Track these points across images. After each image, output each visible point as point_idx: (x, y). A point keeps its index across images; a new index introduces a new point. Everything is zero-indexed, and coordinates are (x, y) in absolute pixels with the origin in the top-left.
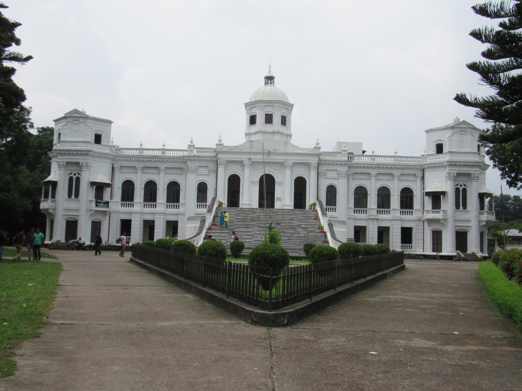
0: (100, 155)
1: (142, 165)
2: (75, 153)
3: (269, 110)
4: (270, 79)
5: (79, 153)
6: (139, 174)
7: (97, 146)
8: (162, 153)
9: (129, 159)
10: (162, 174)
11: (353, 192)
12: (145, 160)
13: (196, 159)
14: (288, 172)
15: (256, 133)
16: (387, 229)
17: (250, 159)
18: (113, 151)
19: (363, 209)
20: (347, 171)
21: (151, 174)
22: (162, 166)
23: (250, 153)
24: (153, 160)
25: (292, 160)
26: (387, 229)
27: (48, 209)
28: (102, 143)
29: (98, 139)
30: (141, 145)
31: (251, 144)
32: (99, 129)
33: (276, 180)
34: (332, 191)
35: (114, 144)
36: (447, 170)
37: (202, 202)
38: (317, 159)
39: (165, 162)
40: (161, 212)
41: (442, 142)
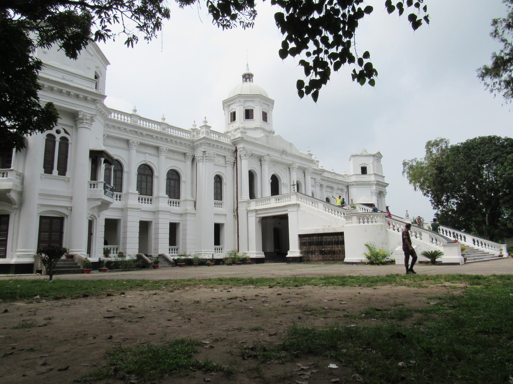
2: (73, 92)
5: (81, 95)
9: (122, 127)
10: (163, 157)
12: (145, 133)
13: (216, 144)
15: (256, 129)
21: (147, 155)
24: (155, 135)
25: (298, 163)
27: (9, 191)
36: (374, 188)
37: (217, 200)
40: (162, 209)
41: (366, 166)
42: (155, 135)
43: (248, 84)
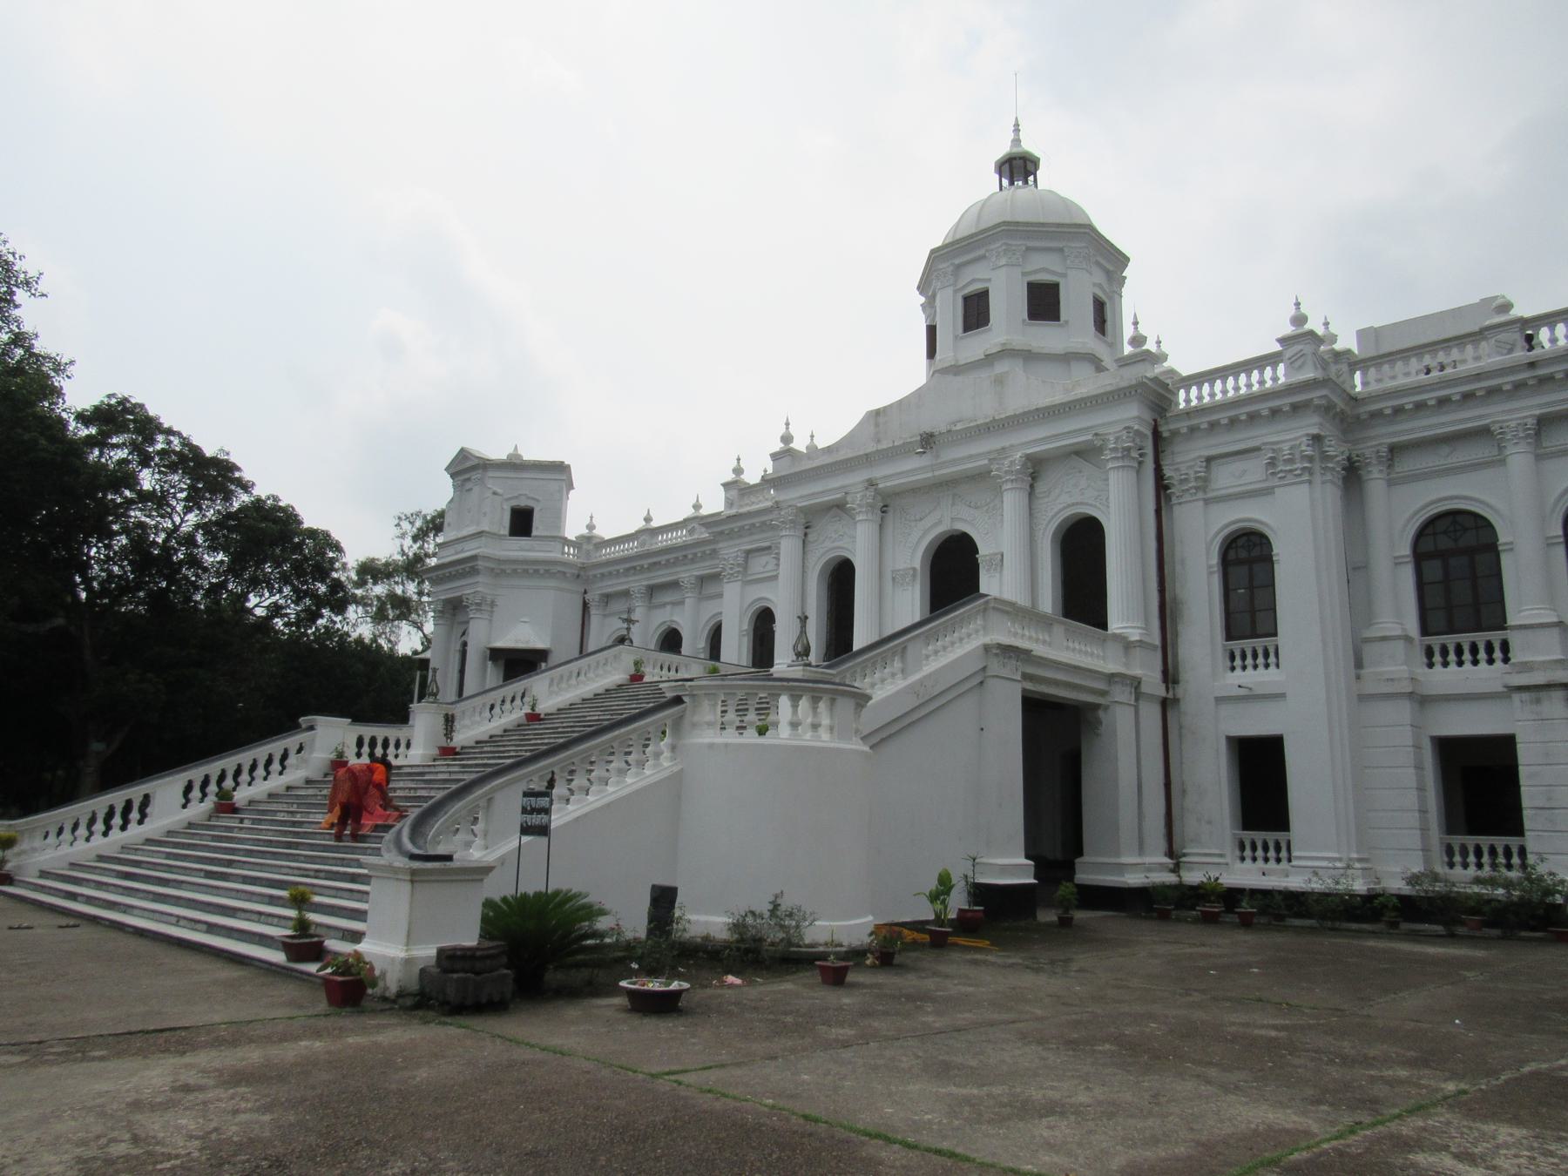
0: (520, 567)
1: (637, 583)
3: (976, 277)
4: (1018, 167)
7: (522, 542)
8: (691, 532)
11: (1406, 550)
14: (1012, 502)
17: (871, 483)
18: (588, 553)
19: (1481, 638)
20: (1317, 439)
21: (668, 607)
22: (686, 574)
23: (867, 460)
28: (534, 533)
29: (522, 522)
30: (648, 519)
31: (877, 425)
32: (525, 492)
33: (984, 550)
34: (1247, 556)
35: (596, 532)
38: (1132, 414)
39: (693, 561)
42: (663, 559)
43: (1021, 192)
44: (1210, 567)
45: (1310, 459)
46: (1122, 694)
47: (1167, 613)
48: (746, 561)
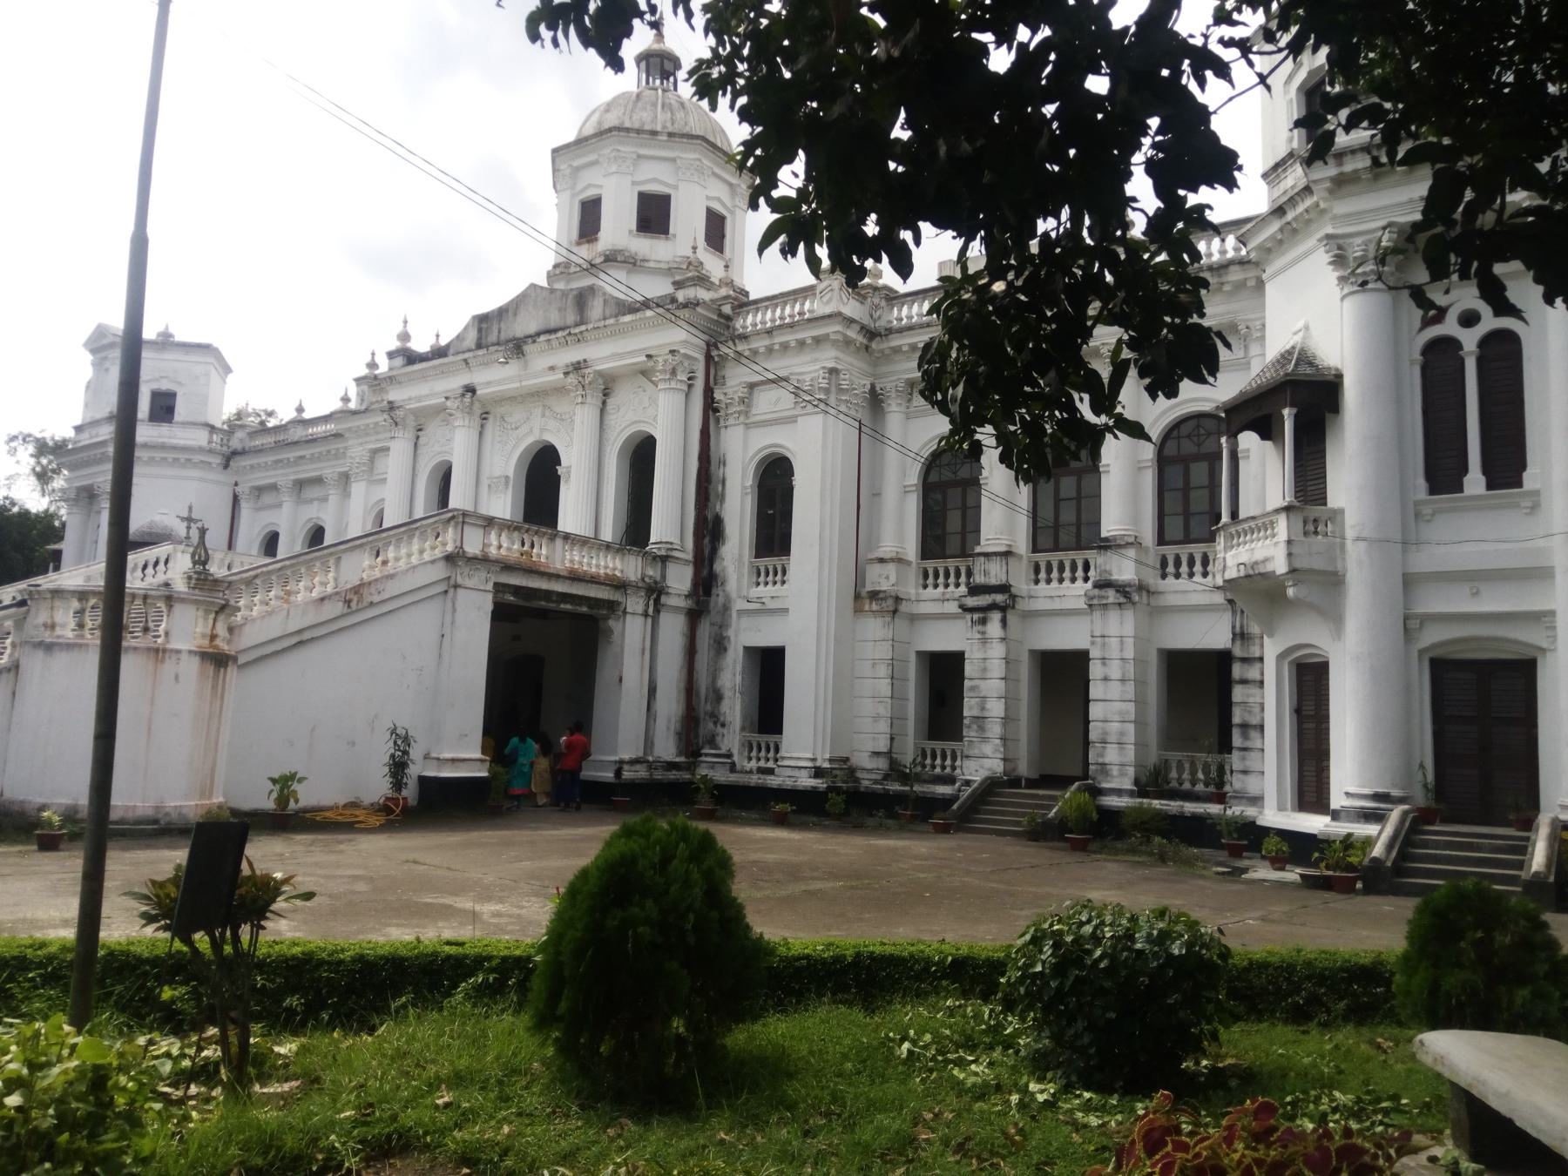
6: (288, 507)
14: (585, 416)
16: (1079, 660)
17: (471, 389)
20: (833, 372)
26: (1079, 660)
28: (177, 418)
30: (300, 410)
44: (744, 488)
45: (827, 391)
46: (635, 603)
47: (709, 530)
48: (372, 460)
